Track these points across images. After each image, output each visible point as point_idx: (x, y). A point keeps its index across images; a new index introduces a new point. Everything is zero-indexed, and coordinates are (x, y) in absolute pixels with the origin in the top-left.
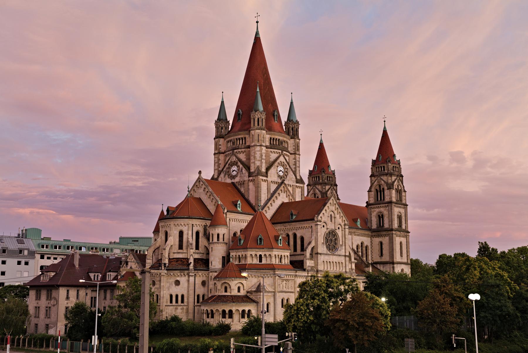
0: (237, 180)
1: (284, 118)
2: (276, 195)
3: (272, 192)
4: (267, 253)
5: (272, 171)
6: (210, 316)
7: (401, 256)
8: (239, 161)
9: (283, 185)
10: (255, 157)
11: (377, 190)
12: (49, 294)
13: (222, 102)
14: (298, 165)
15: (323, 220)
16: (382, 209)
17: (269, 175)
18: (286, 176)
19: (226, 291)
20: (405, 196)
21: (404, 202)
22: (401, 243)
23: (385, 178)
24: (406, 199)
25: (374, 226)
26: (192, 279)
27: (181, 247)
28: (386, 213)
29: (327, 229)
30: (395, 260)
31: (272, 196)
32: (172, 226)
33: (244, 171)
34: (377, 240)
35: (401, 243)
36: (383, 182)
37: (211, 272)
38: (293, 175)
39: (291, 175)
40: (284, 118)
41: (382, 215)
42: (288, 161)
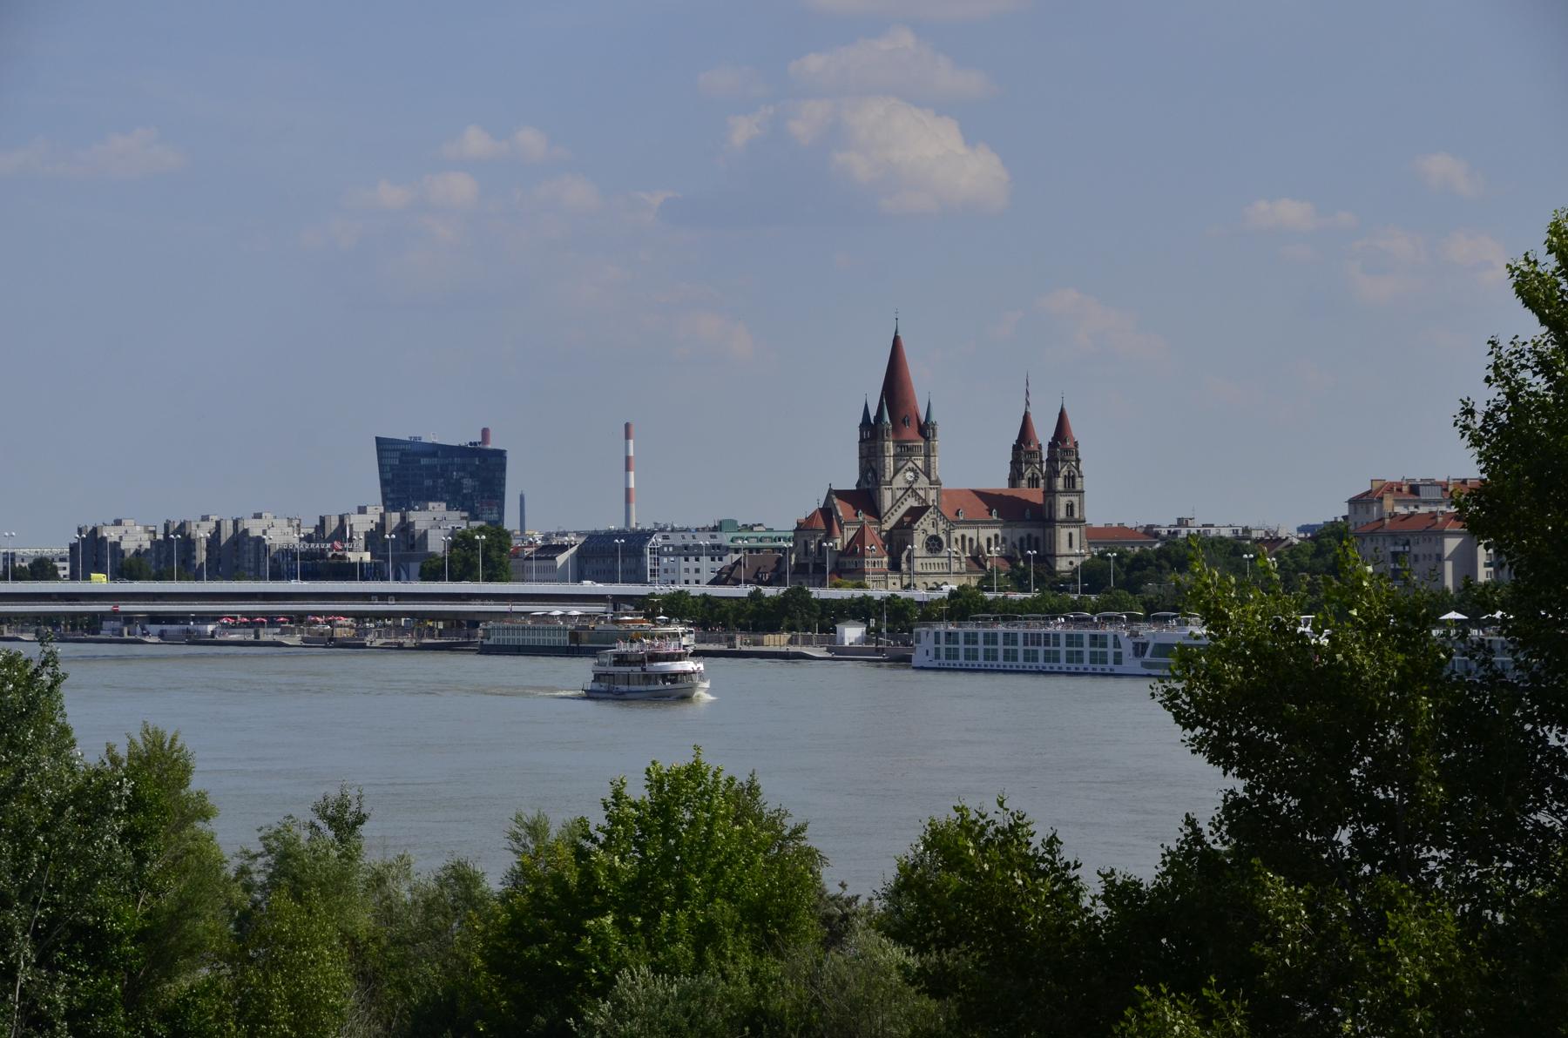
0: (870, 487)
1: (923, 418)
2: (902, 500)
3: (898, 498)
5: (899, 477)
7: (1071, 545)
9: (910, 490)
13: (866, 405)
14: (932, 466)
15: (922, 527)
17: (894, 482)
18: (916, 480)
20: (1082, 482)
21: (1078, 487)
22: (1070, 535)
24: (1082, 485)
25: (1047, 517)
29: (927, 535)
30: (1057, 553)
31: (896, 503)
34: (1048, 531)
35: (1070, 535)
38: (926, 478)
39: (923, 478)
40: (923, 418)
42: (920, 467)
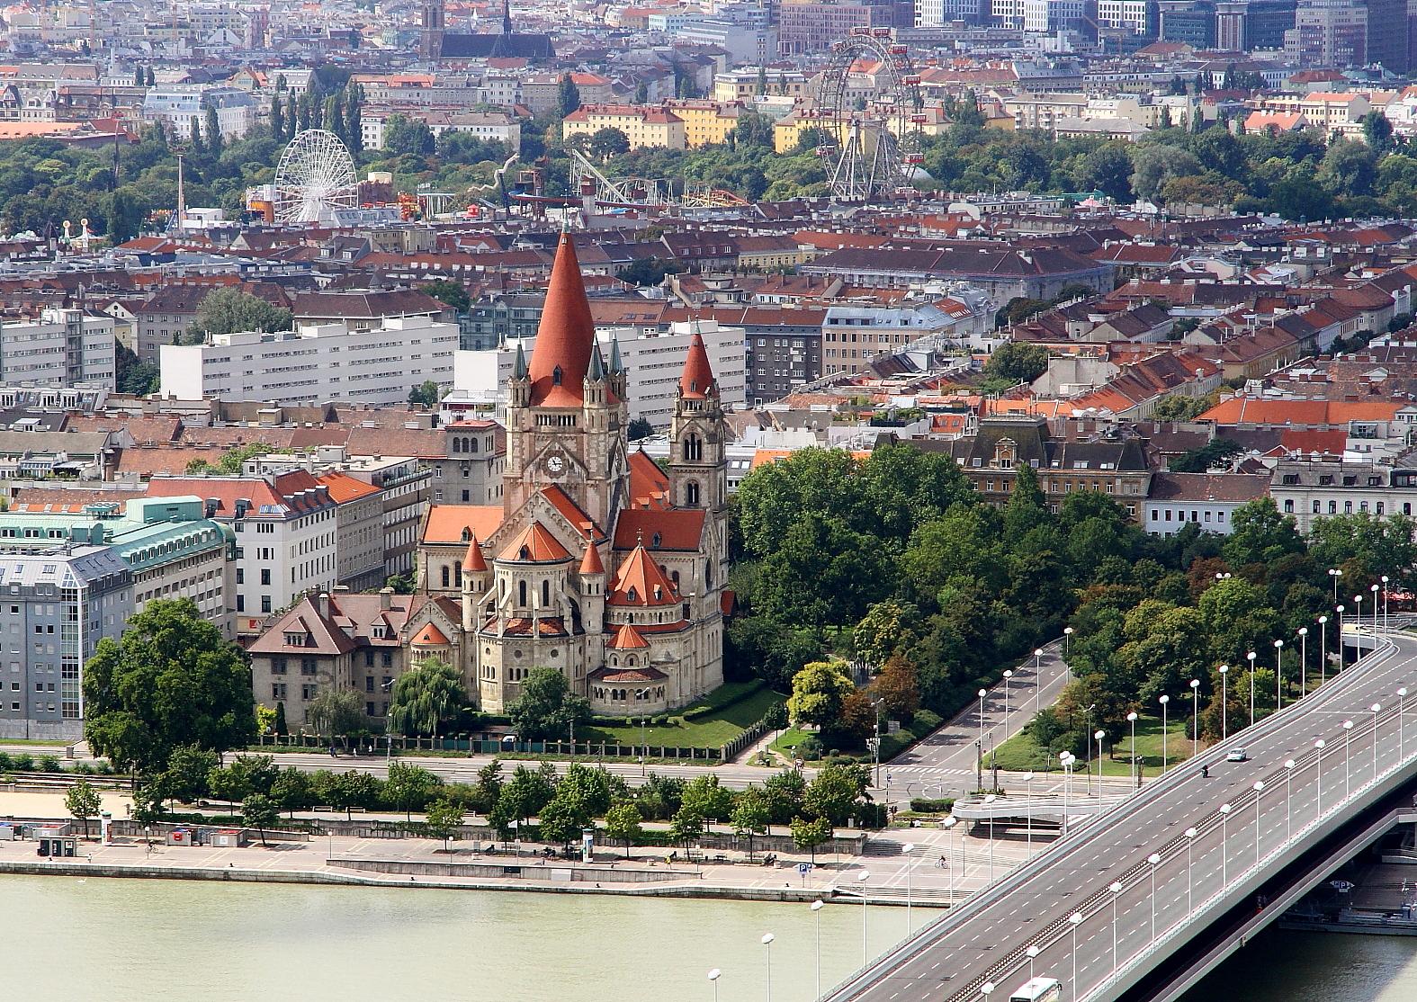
0: (563, 480)
4: (669, 611)
6: (619, 697)
8: (567, 451)
10: (598, 452)
11: (686, 441)
12: (309, 666)
16: (696, 476)
19: (632, 664)
23: (704, 423)
26: (571, 646)
27: (546, 603)
28: (703, 482)
32: (535, 574)
33: (577, 468)
36: (699, 429)
37: (592, 635)
41: (697, 486)
